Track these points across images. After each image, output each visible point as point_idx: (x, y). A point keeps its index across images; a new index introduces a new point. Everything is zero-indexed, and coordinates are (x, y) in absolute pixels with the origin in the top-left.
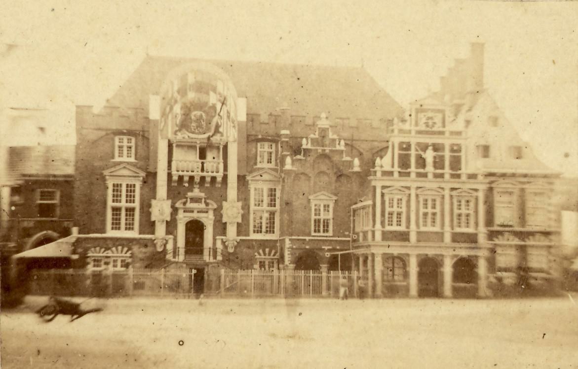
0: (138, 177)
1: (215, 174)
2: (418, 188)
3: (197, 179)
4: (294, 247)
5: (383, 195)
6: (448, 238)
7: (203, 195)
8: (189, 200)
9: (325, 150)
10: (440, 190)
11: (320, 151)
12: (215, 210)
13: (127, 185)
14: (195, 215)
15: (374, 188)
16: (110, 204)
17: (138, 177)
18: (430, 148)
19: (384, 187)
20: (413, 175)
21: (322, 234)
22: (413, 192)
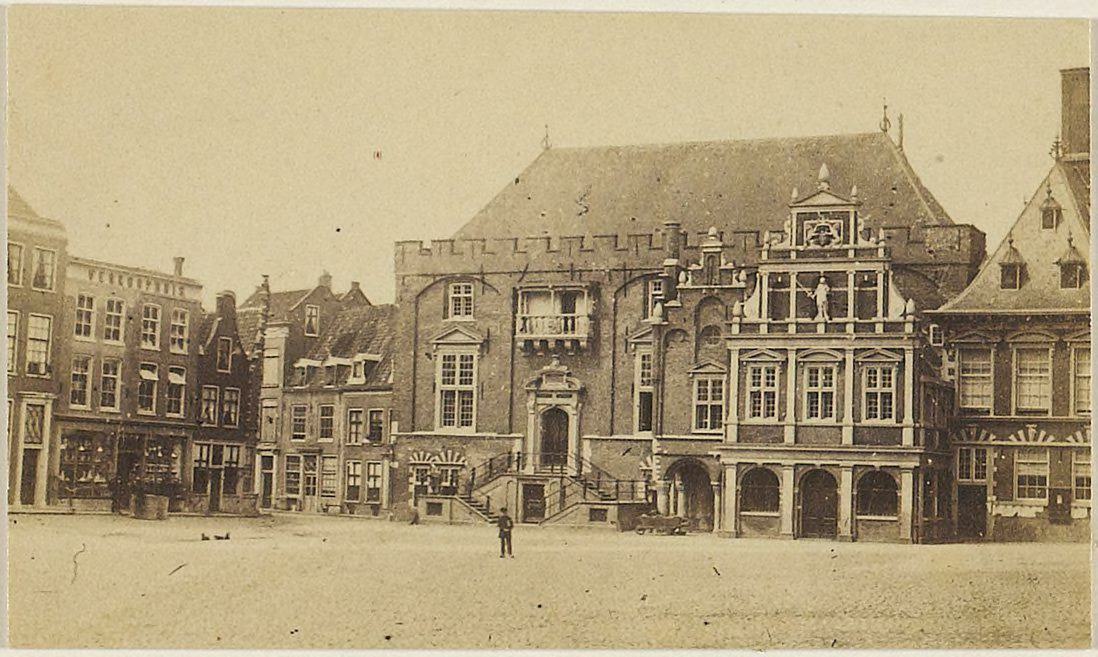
0: (475, 344)
1: (576, 335)
2: (798, 351)
3: (552, 345)
4: (665, 452)
5: (740, 363)
6: (847, 436)
7: (564, 369)
8: (544, 377)
9: (713, 289)
10: (836, 353)
11: (704, 291)
12: (582, 392)
13: (462, 356)
14: (554, 401)
15: (729, 351)
16: (440, 386)
17: (475, 344)
18: (822, 280)
19: (741, 352)
20: (792, 329)
21: (708, 430)
22: (792, 357)
